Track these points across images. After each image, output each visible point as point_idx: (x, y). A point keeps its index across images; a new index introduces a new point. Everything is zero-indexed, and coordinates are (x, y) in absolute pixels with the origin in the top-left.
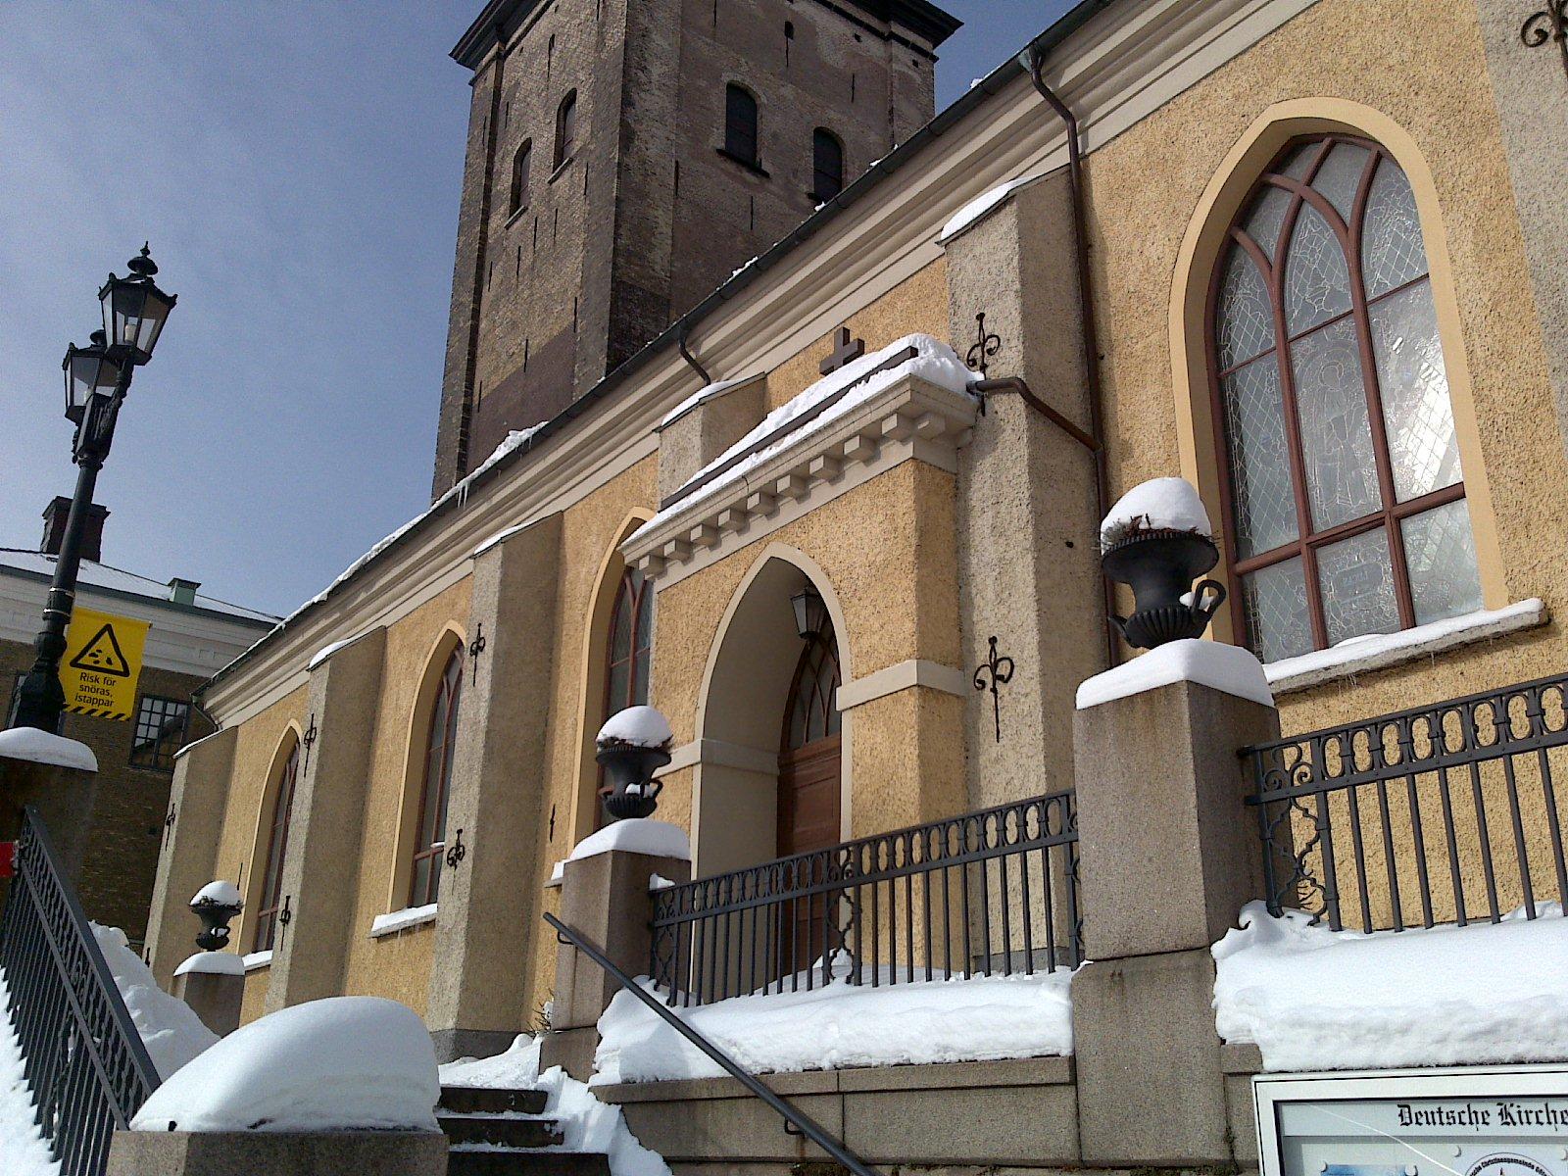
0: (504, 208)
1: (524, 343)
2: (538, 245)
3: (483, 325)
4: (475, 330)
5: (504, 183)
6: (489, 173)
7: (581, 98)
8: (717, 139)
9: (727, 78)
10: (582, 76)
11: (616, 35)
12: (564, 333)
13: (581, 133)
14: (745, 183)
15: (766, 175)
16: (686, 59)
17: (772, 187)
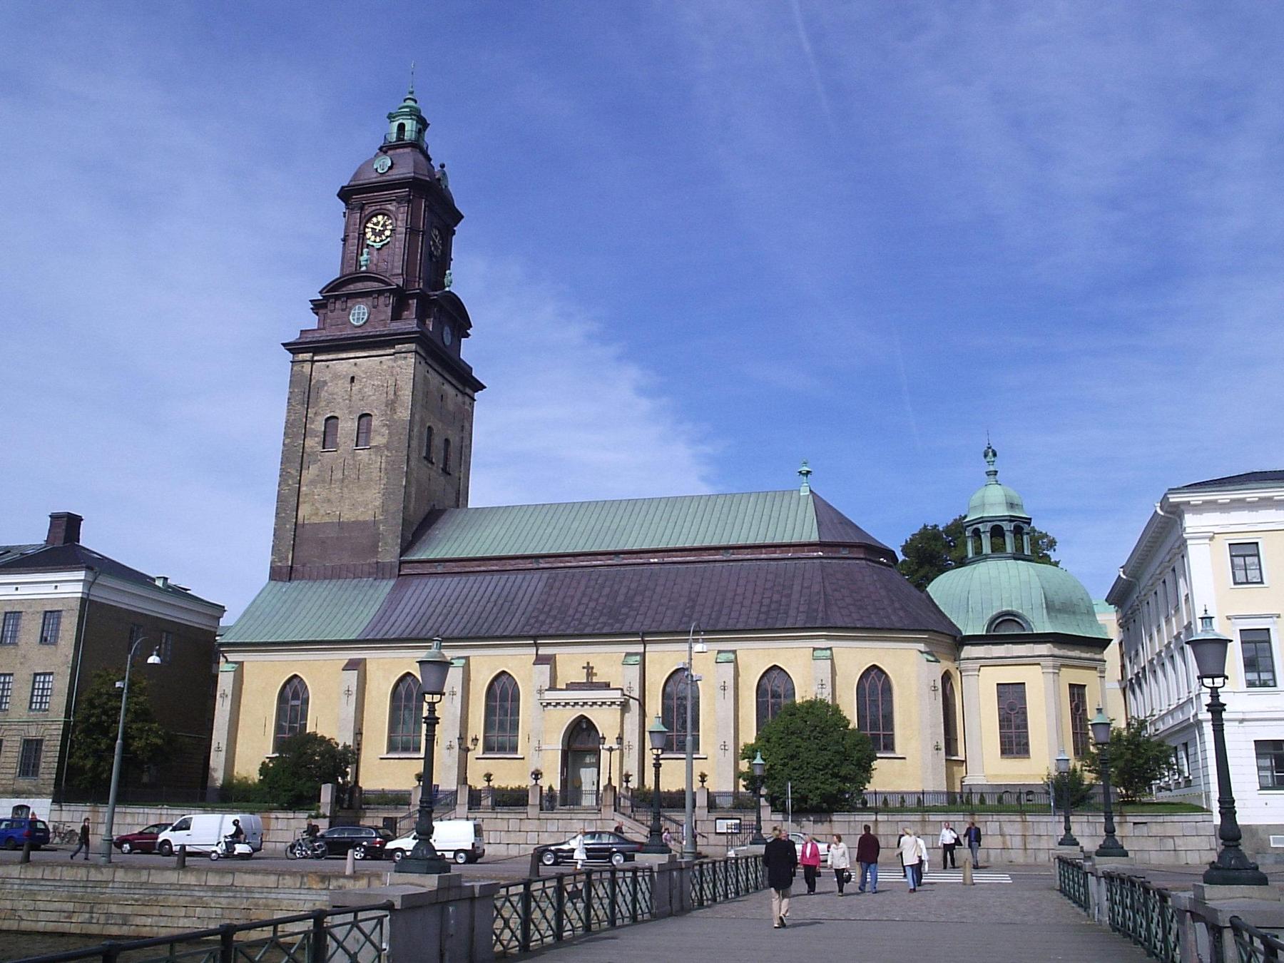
0: (319, 439)
1: (338, 513)
2: (346, 473)
3: (303, 489)
4: (299, 488)
5: (319, 425)
6: (306, 417)
7: (375, 422)
8: (424, 454)
9: (428, 424)
10: (375, 412)
11: (404, 414)
12: (365, 523)
13: (378, 440)
14: (428, 467)
15: (433, 463)
16: (422, 421)
17: (435, 468)
